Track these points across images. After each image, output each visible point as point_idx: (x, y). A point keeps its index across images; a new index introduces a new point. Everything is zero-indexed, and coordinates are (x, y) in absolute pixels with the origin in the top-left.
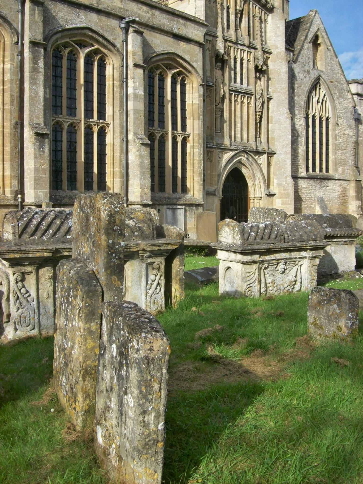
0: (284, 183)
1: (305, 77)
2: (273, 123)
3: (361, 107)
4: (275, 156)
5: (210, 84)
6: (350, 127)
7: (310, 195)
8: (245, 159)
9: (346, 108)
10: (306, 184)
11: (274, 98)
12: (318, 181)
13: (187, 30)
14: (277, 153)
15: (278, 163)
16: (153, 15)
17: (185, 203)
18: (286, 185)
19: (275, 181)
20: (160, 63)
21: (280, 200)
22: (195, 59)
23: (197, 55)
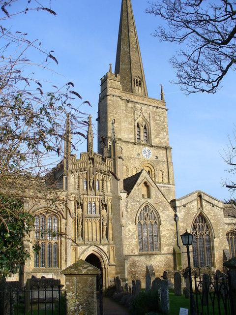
3: (180, 213)
5: (74, 216)
6: (172, 225)
9: (168, 215)
12: (148, 256)
20: (41, 212)
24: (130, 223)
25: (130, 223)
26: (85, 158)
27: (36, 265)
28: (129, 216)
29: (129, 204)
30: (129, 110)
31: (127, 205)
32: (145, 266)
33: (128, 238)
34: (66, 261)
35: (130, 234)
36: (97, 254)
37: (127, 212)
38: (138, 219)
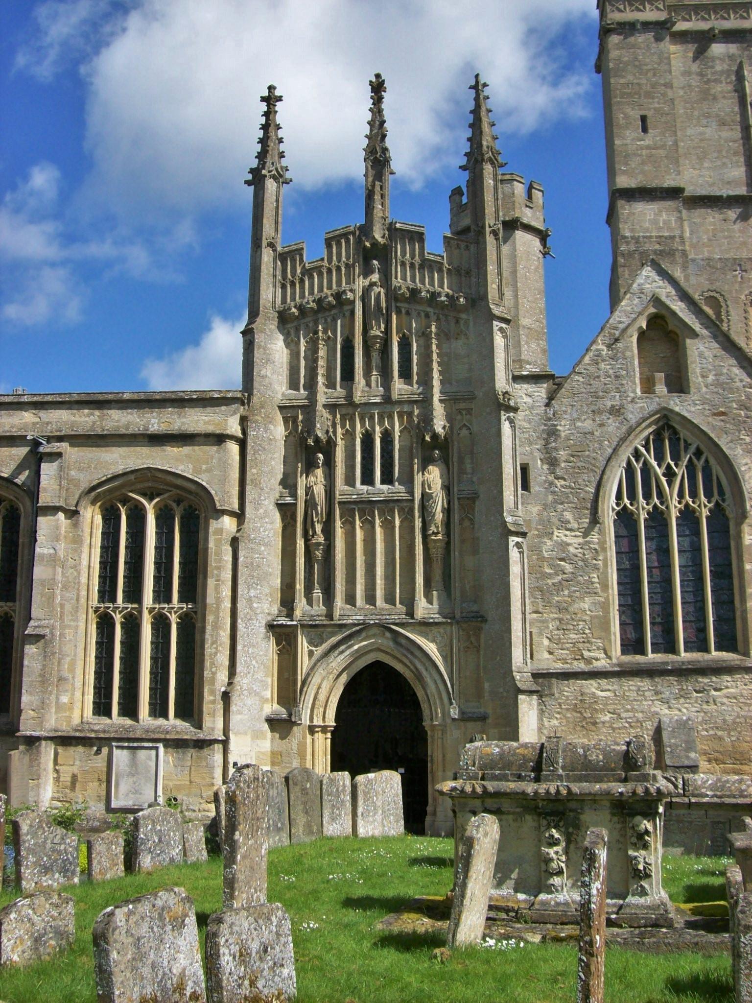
0: (501, 690)
1: (602, 425)
2: (481, 551)
4: (486, 627)
5: (289, 500)
7: (630, 714)
8: (391, 644)
10: (616, 687)
11: (482, 496)
13: (184, 420)
14: (489, 619)
15: (490, 642)
16: (101, 418)
17: (163, 736)
18: (505, 694)
19: (487, 685)
21: (496, 731)
22: (204, 467)
23: (212, 457)
24: (568, 516)
25: (568, 516)
26: (344, 253)
27: (102, 708)
28: (559, 483)
29: (564, 428)
30: (718, 68)
31: (552, 433)
32: (650, 726)
33: (559, 587)
34: (226, 697)
35: (568, 568)
36: (399, 667)
37: (552, 463)
38: (619, 497)
